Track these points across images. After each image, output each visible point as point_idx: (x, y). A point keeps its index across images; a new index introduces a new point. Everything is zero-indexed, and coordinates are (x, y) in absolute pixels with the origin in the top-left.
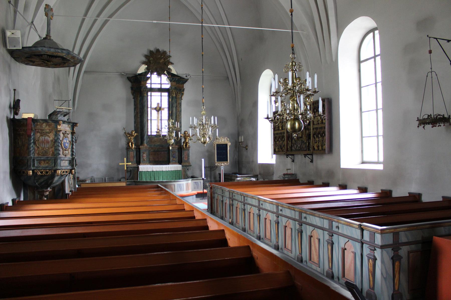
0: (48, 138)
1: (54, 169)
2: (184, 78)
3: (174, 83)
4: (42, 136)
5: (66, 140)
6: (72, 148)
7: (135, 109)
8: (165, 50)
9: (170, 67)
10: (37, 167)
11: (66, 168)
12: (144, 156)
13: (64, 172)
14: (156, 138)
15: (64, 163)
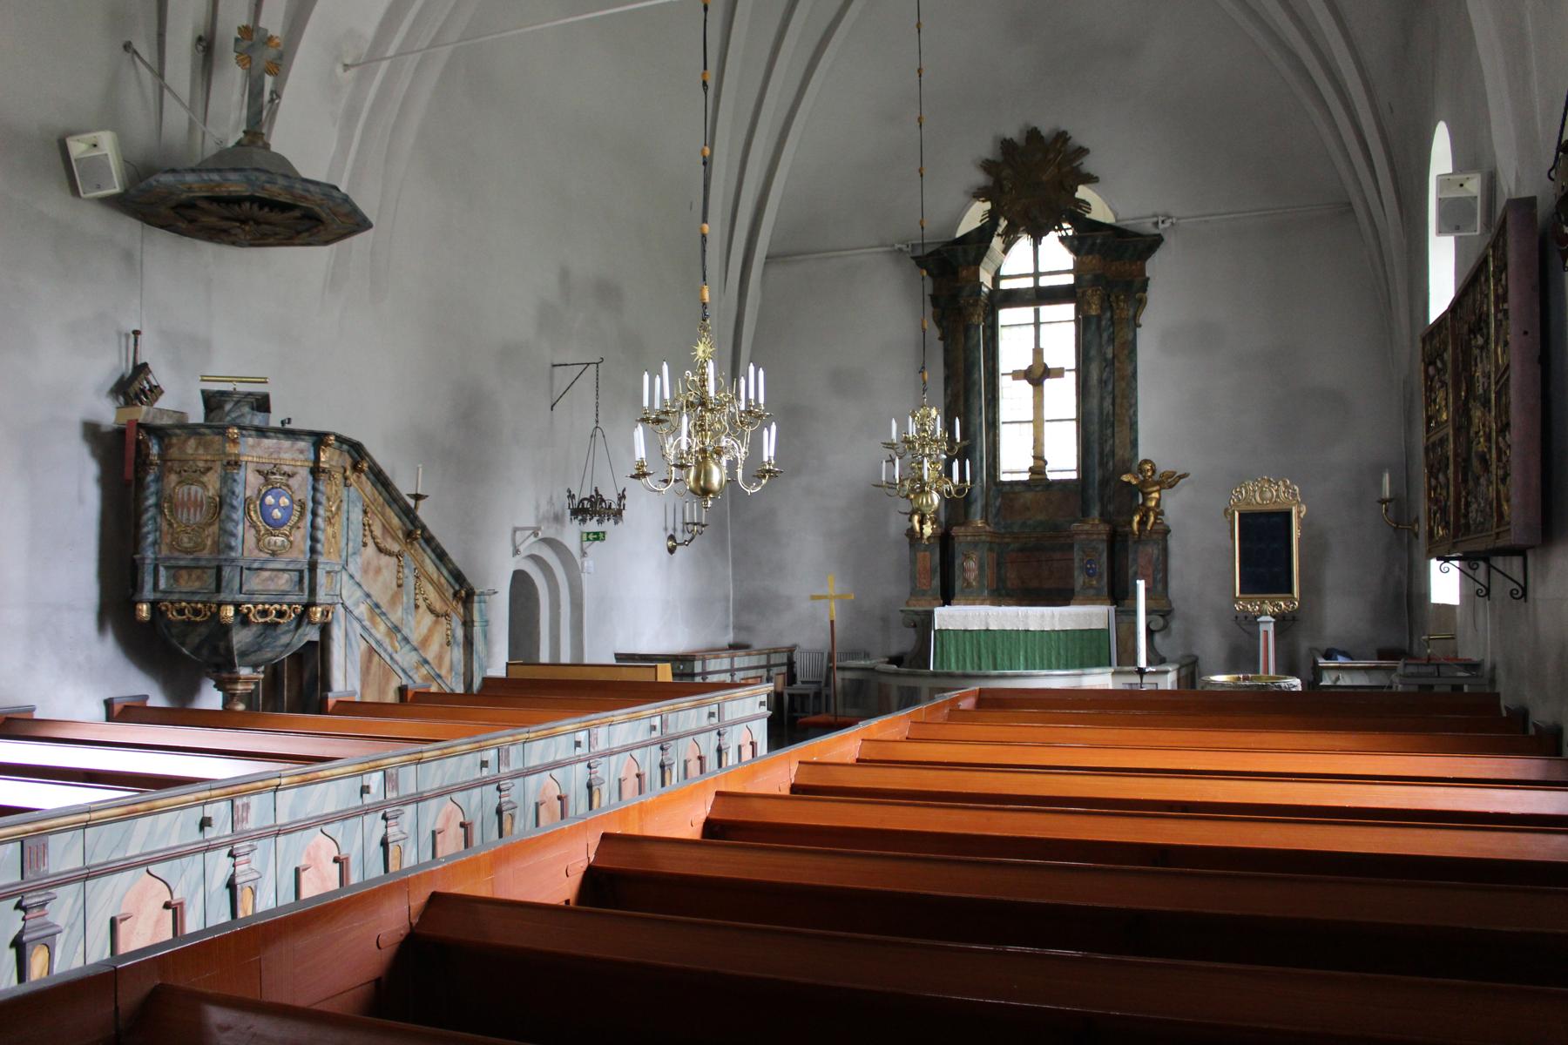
0: (200, 491)
2: (1138, 235)
3: (1093, 261)
4: (179, 483)
5: (277, 498)
6: (313, 526)
7: (947, 380)
8: (1063, 128)
9: (1083, 192)
10: (164, 592)
11: (273, 599)
12: (970, 567)
13: (265, 613)
14: (1029, 496)
15: (270, 579)
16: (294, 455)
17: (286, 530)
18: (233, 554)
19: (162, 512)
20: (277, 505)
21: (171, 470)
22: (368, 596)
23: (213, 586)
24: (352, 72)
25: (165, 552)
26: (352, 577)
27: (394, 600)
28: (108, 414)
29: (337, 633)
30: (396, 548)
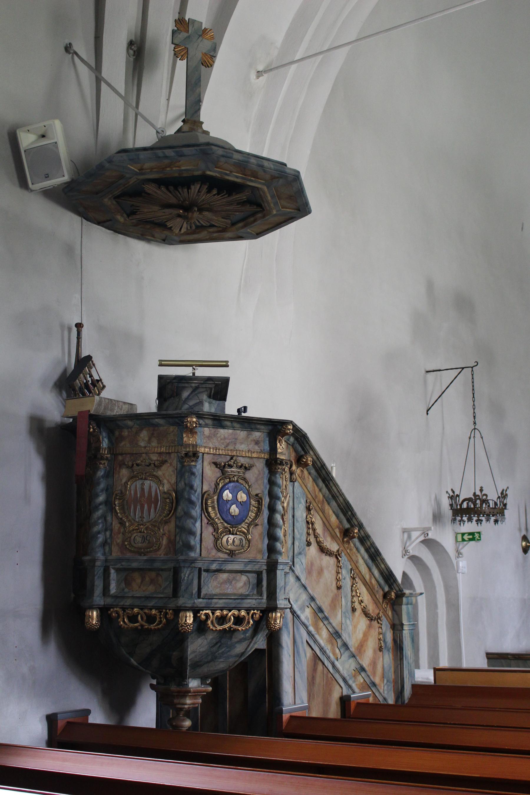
0: (154, 486)
1: (172, 605)
10: (115, 597)
13: (222, 620)
16: (248, 447)
17: (243, 527)
18: (192, 554)
19: (112, 509)
20: (235, 500)
21: (122, 464)
22: (312, 599)
23: (170, 591)
24: (263, 79)
25: (116, 553)
26: (298, 579)
27: (334, 603)
28: (54, 410)
29: (286, 640)
30: (334, 547)
